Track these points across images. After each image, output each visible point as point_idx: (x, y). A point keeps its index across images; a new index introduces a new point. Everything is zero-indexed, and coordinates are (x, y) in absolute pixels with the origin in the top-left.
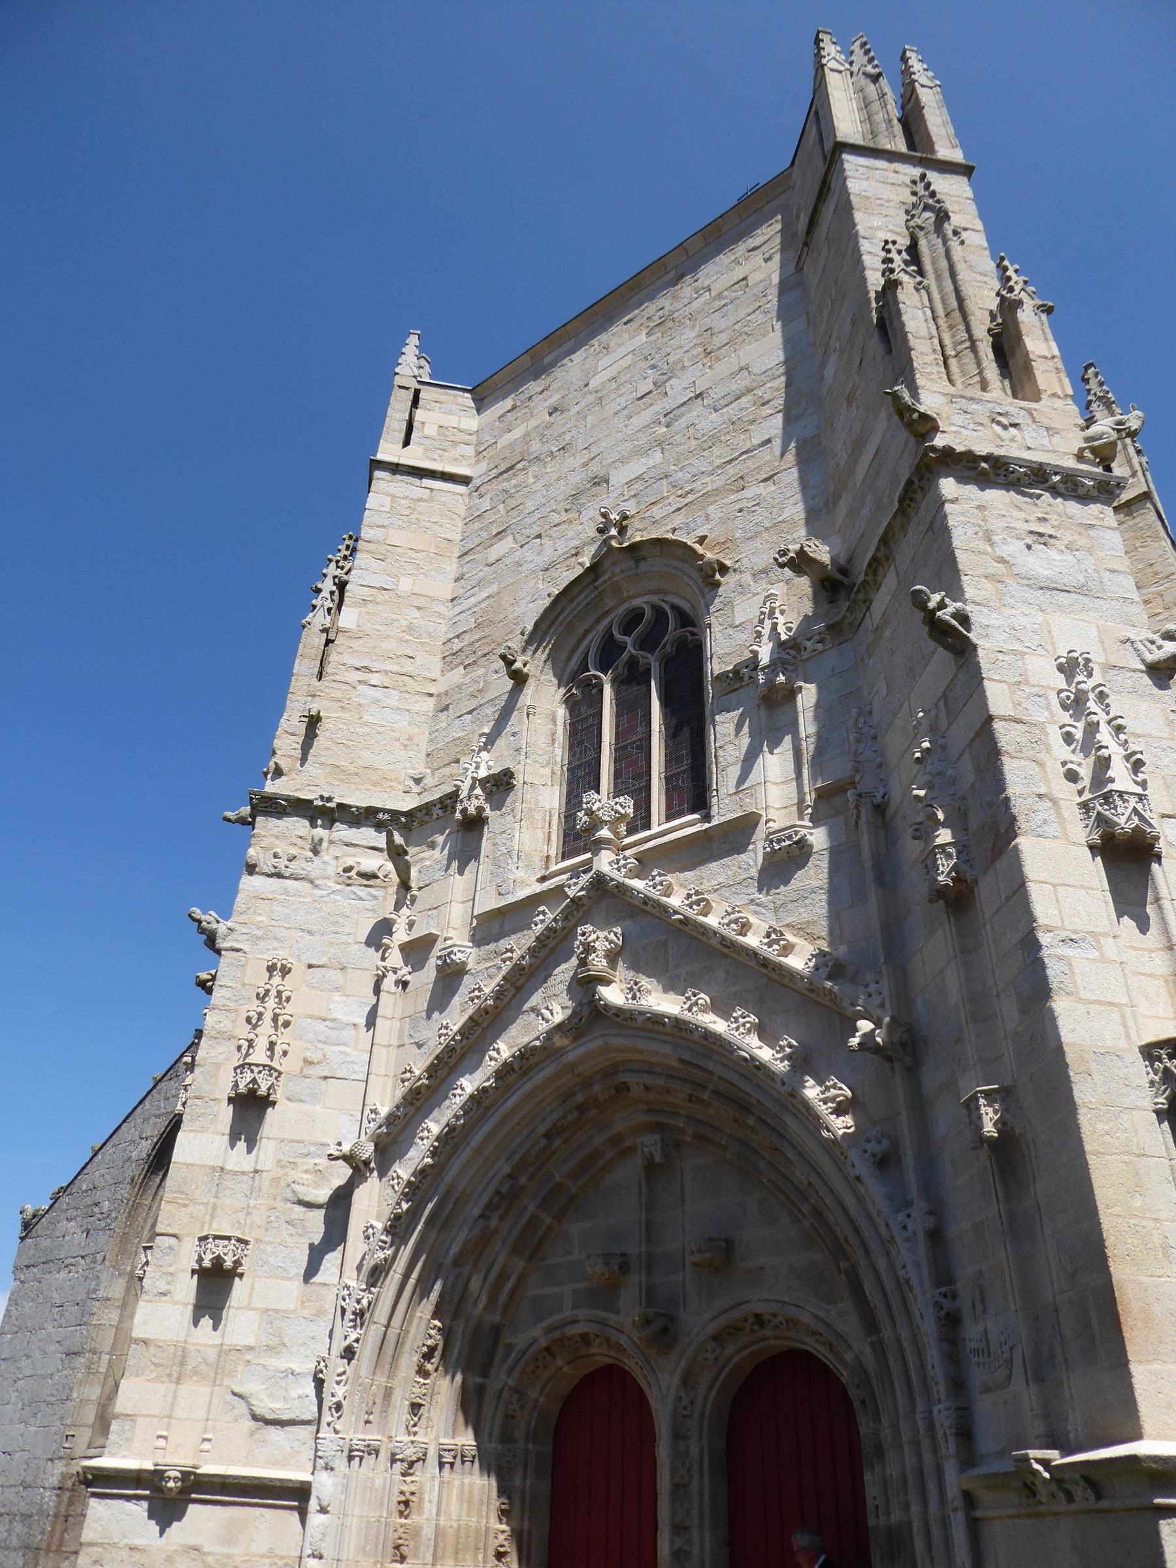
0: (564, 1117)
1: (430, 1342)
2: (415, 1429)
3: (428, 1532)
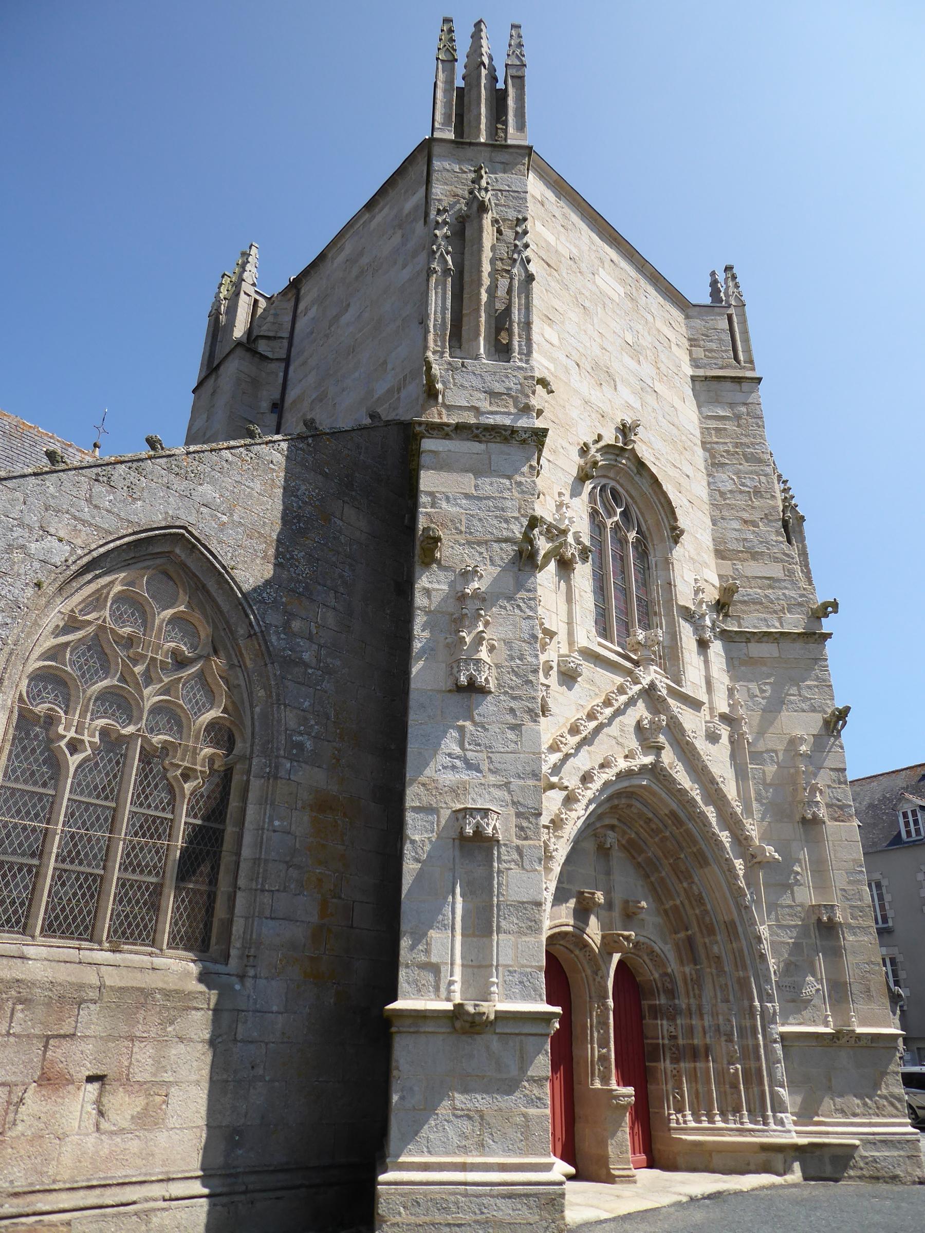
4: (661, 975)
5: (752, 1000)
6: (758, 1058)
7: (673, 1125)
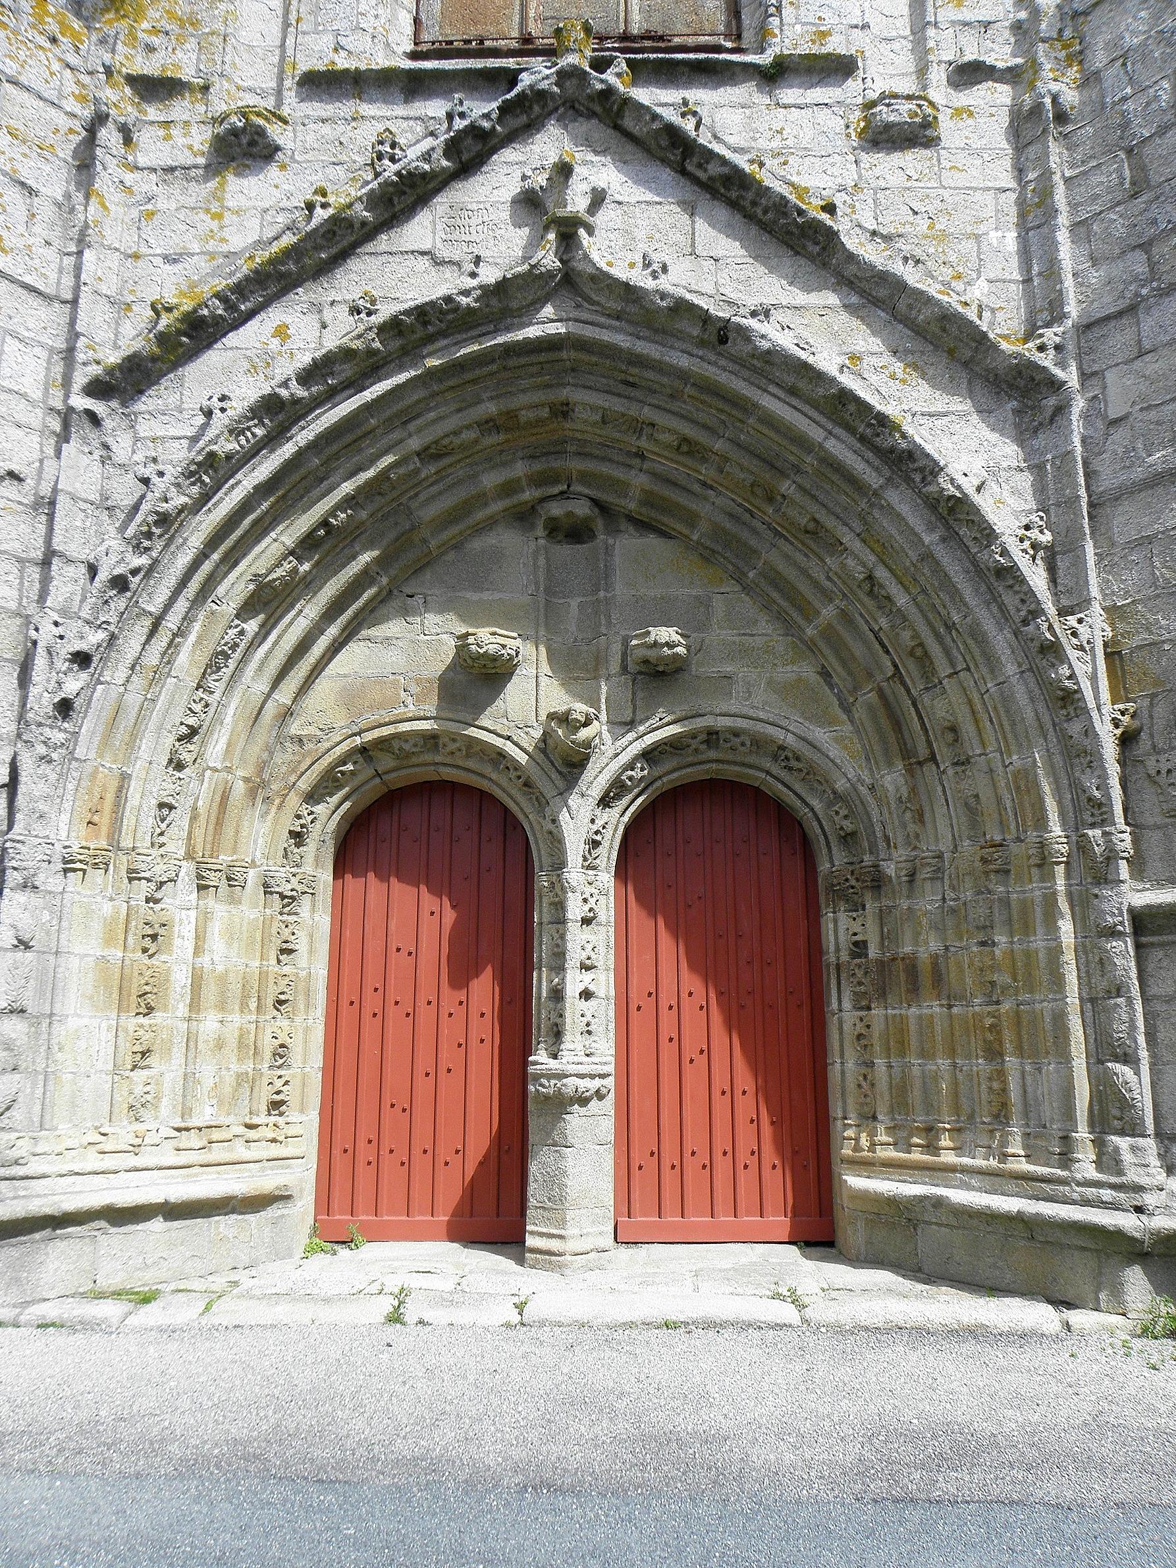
0: (456, 433)
1: (191, 721)
2: (162, 839)
3: (181, 978)
4: (830, 804)
5: (1041, 822)
6: (1058, 982)
7: (847, 1152)
